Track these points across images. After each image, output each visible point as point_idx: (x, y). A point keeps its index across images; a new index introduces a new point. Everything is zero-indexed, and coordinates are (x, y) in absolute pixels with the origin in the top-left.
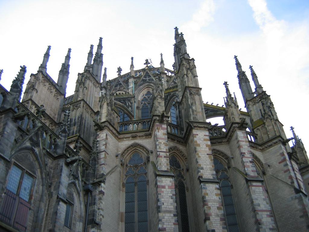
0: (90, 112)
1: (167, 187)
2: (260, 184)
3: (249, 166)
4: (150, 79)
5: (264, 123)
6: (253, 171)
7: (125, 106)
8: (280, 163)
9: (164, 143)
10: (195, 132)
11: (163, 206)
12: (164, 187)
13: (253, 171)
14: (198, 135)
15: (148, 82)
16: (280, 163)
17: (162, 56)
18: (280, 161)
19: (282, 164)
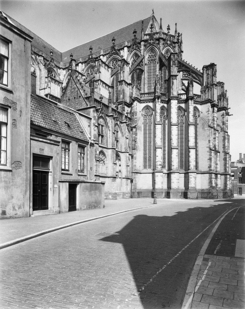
0: (126, 85)
1: (159, 129)
2: (193, 126)
3: (191, 118)
4: (153, 42)
5: (205, 91)
6: (192, 120)
7: (140, 67)
8: (206, 112)
9: (159, 109)
10: (172, 101)
11: (157, 136)
12: (158, 129)
13: (192, 120)
14: (173, 103)
15: (152, 45)
16: (206, 112)
17: (161, 21)
18: (207, 111)
19: (207, 113)
